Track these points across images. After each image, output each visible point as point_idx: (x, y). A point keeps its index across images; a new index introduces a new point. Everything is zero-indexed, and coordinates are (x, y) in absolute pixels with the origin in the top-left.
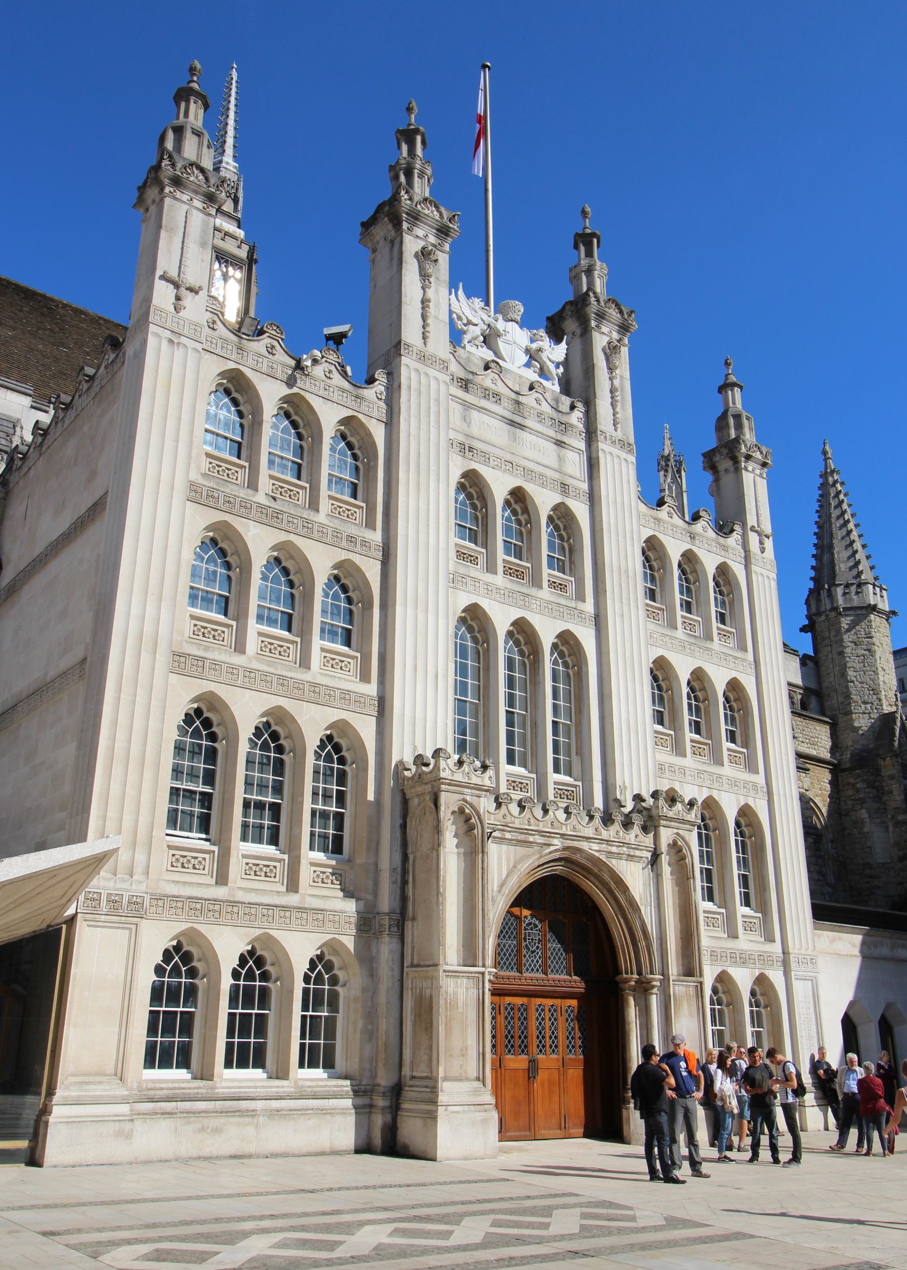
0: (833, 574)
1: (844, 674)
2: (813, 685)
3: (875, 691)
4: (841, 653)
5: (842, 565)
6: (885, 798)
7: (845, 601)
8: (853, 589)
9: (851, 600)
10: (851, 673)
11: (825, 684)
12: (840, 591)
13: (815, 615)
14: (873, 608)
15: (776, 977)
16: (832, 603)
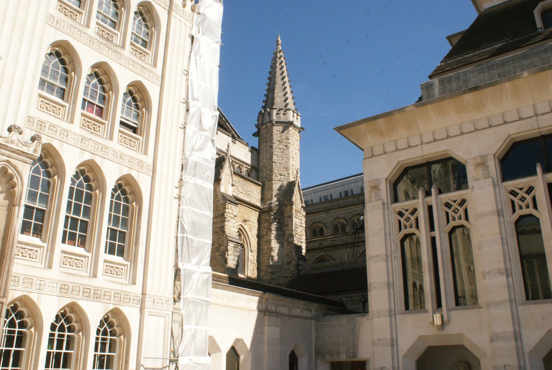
0: (273, 104)
1: (271, 158)
2: (255, 165)
3: (287, 169)
4: (271, 147)
5: (278, 99)
6: (285, 228)
7: (277, 117)
8: (282, 112)
9: (280, 117)
10: (275, 158)
11: (261, 164)
12: (275, 112)
13: (260, 125)
14: (291, 124)
15: (131, 313)
16: (270, 118)
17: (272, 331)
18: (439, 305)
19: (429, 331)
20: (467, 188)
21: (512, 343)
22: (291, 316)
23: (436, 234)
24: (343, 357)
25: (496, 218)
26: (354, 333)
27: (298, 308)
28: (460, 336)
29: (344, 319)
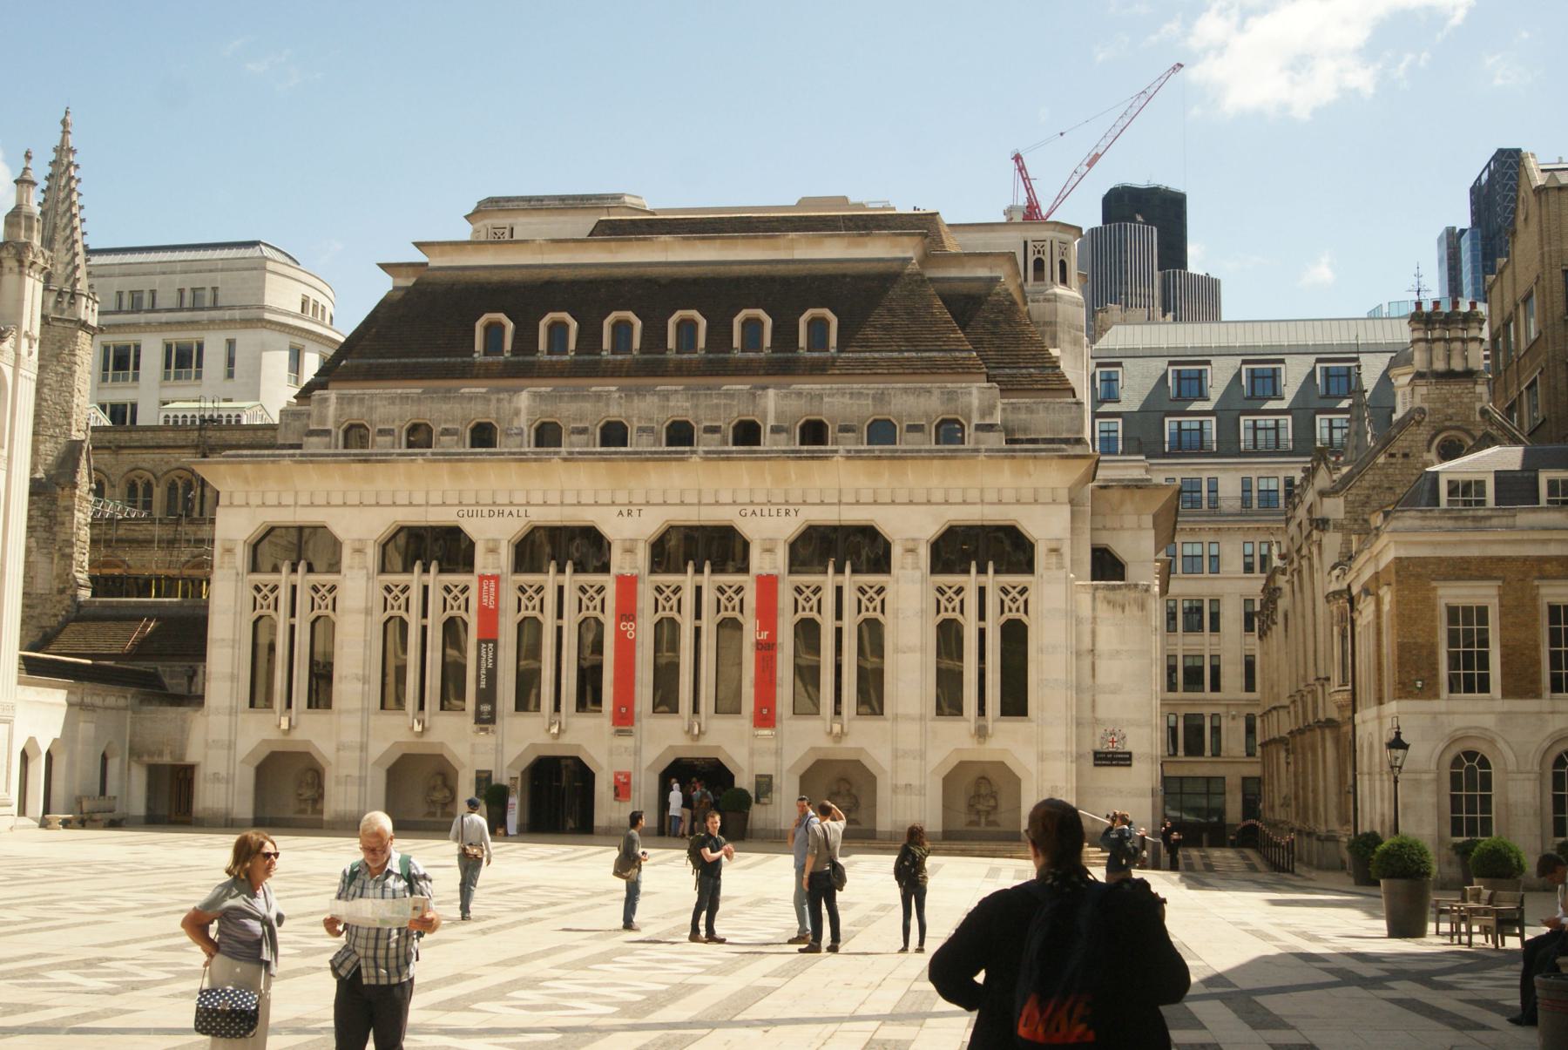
3: (67, 415)
6: (56, 529)
8: (67, 298)
17: (86, 728)
18: (289, 706)
19: (274, 735)
20: (339, 572)
21: (357, 754)
22: (106, 708)
23: (297, 621)
24: (167, 759)
25: (363, 617)
26: (184, 731)
27: (112, 698)
28: (308, 742)
29: (172, 713)
